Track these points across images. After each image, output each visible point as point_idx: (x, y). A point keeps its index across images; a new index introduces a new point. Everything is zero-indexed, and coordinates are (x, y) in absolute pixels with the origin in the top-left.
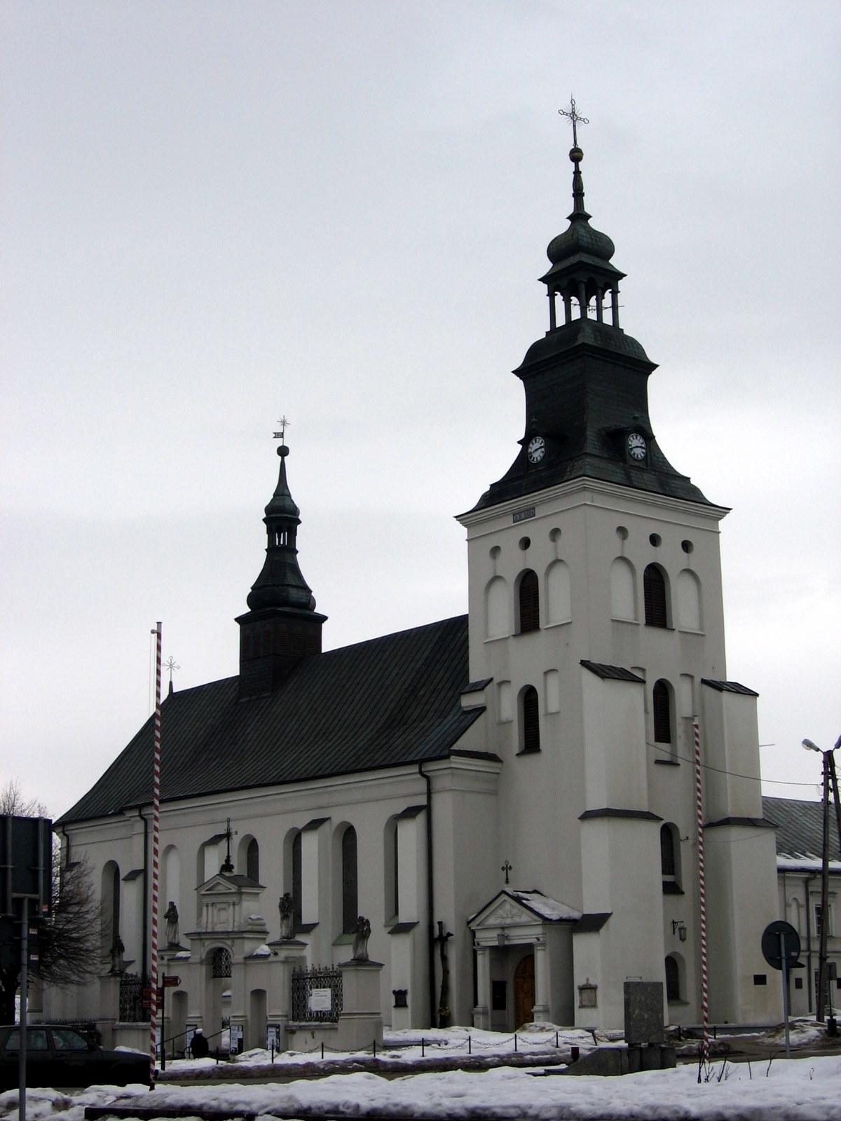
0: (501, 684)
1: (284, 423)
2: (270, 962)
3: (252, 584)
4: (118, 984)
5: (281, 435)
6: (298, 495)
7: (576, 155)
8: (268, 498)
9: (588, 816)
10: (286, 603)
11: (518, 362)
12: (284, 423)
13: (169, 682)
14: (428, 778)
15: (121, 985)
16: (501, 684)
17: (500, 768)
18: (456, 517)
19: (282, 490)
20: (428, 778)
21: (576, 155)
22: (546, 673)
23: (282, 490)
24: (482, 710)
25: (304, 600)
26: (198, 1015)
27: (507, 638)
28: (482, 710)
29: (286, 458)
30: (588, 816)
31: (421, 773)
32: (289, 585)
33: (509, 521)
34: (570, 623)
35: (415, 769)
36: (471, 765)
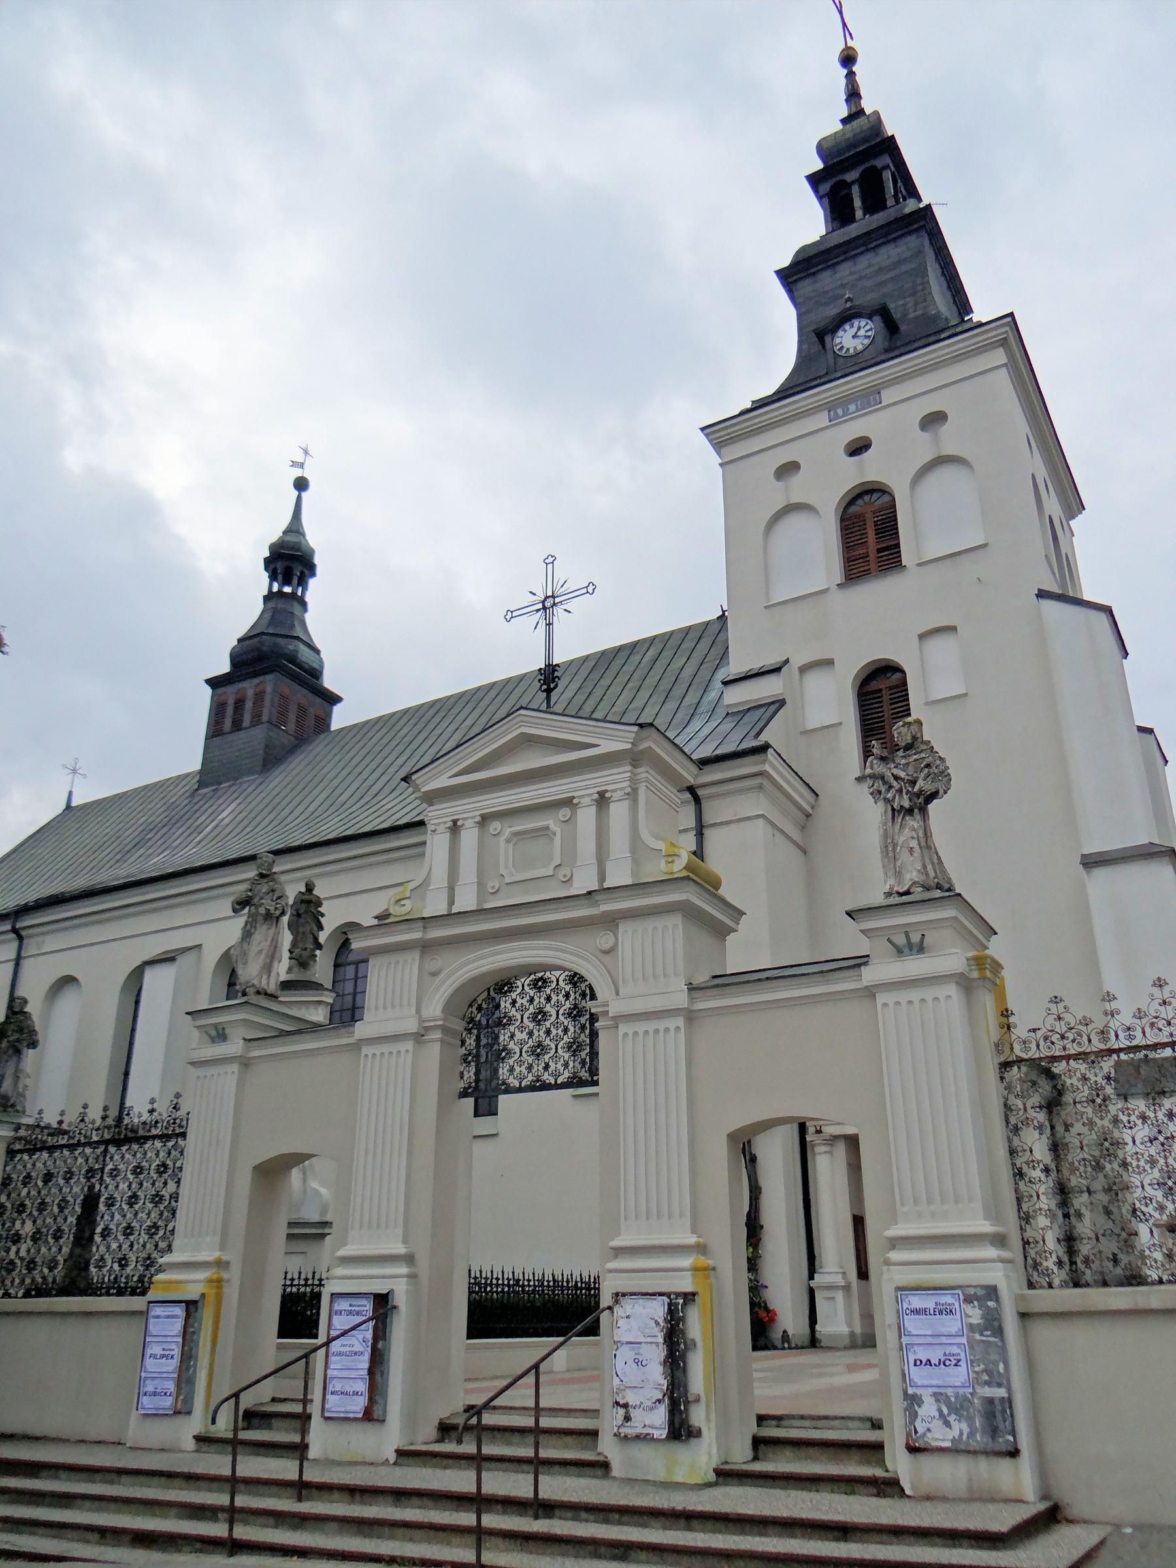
0: (804, 669)
1: (306, 452)
3: (242, 631)
5: (301, 465)
6: (314, 537)
7: (848, 59)
9: (1091, 862)
10: (293, 659)
11: (785, 262)
12: (306, 452)
13: (69, 789)
16: (804, 669)
17: (813, 808)
18: (702, 429)
20: (697, 800)
21: (848, 59)
22: (923, 637)
24: (782, 703)
25: (315, 665)
26: (400, 1249)
28: (782, 703)
29: (304, 494)
30: (1091, 862)
32: (297, 638)
33: (822, 419)
34: (985, 546)
36: (788, 782)
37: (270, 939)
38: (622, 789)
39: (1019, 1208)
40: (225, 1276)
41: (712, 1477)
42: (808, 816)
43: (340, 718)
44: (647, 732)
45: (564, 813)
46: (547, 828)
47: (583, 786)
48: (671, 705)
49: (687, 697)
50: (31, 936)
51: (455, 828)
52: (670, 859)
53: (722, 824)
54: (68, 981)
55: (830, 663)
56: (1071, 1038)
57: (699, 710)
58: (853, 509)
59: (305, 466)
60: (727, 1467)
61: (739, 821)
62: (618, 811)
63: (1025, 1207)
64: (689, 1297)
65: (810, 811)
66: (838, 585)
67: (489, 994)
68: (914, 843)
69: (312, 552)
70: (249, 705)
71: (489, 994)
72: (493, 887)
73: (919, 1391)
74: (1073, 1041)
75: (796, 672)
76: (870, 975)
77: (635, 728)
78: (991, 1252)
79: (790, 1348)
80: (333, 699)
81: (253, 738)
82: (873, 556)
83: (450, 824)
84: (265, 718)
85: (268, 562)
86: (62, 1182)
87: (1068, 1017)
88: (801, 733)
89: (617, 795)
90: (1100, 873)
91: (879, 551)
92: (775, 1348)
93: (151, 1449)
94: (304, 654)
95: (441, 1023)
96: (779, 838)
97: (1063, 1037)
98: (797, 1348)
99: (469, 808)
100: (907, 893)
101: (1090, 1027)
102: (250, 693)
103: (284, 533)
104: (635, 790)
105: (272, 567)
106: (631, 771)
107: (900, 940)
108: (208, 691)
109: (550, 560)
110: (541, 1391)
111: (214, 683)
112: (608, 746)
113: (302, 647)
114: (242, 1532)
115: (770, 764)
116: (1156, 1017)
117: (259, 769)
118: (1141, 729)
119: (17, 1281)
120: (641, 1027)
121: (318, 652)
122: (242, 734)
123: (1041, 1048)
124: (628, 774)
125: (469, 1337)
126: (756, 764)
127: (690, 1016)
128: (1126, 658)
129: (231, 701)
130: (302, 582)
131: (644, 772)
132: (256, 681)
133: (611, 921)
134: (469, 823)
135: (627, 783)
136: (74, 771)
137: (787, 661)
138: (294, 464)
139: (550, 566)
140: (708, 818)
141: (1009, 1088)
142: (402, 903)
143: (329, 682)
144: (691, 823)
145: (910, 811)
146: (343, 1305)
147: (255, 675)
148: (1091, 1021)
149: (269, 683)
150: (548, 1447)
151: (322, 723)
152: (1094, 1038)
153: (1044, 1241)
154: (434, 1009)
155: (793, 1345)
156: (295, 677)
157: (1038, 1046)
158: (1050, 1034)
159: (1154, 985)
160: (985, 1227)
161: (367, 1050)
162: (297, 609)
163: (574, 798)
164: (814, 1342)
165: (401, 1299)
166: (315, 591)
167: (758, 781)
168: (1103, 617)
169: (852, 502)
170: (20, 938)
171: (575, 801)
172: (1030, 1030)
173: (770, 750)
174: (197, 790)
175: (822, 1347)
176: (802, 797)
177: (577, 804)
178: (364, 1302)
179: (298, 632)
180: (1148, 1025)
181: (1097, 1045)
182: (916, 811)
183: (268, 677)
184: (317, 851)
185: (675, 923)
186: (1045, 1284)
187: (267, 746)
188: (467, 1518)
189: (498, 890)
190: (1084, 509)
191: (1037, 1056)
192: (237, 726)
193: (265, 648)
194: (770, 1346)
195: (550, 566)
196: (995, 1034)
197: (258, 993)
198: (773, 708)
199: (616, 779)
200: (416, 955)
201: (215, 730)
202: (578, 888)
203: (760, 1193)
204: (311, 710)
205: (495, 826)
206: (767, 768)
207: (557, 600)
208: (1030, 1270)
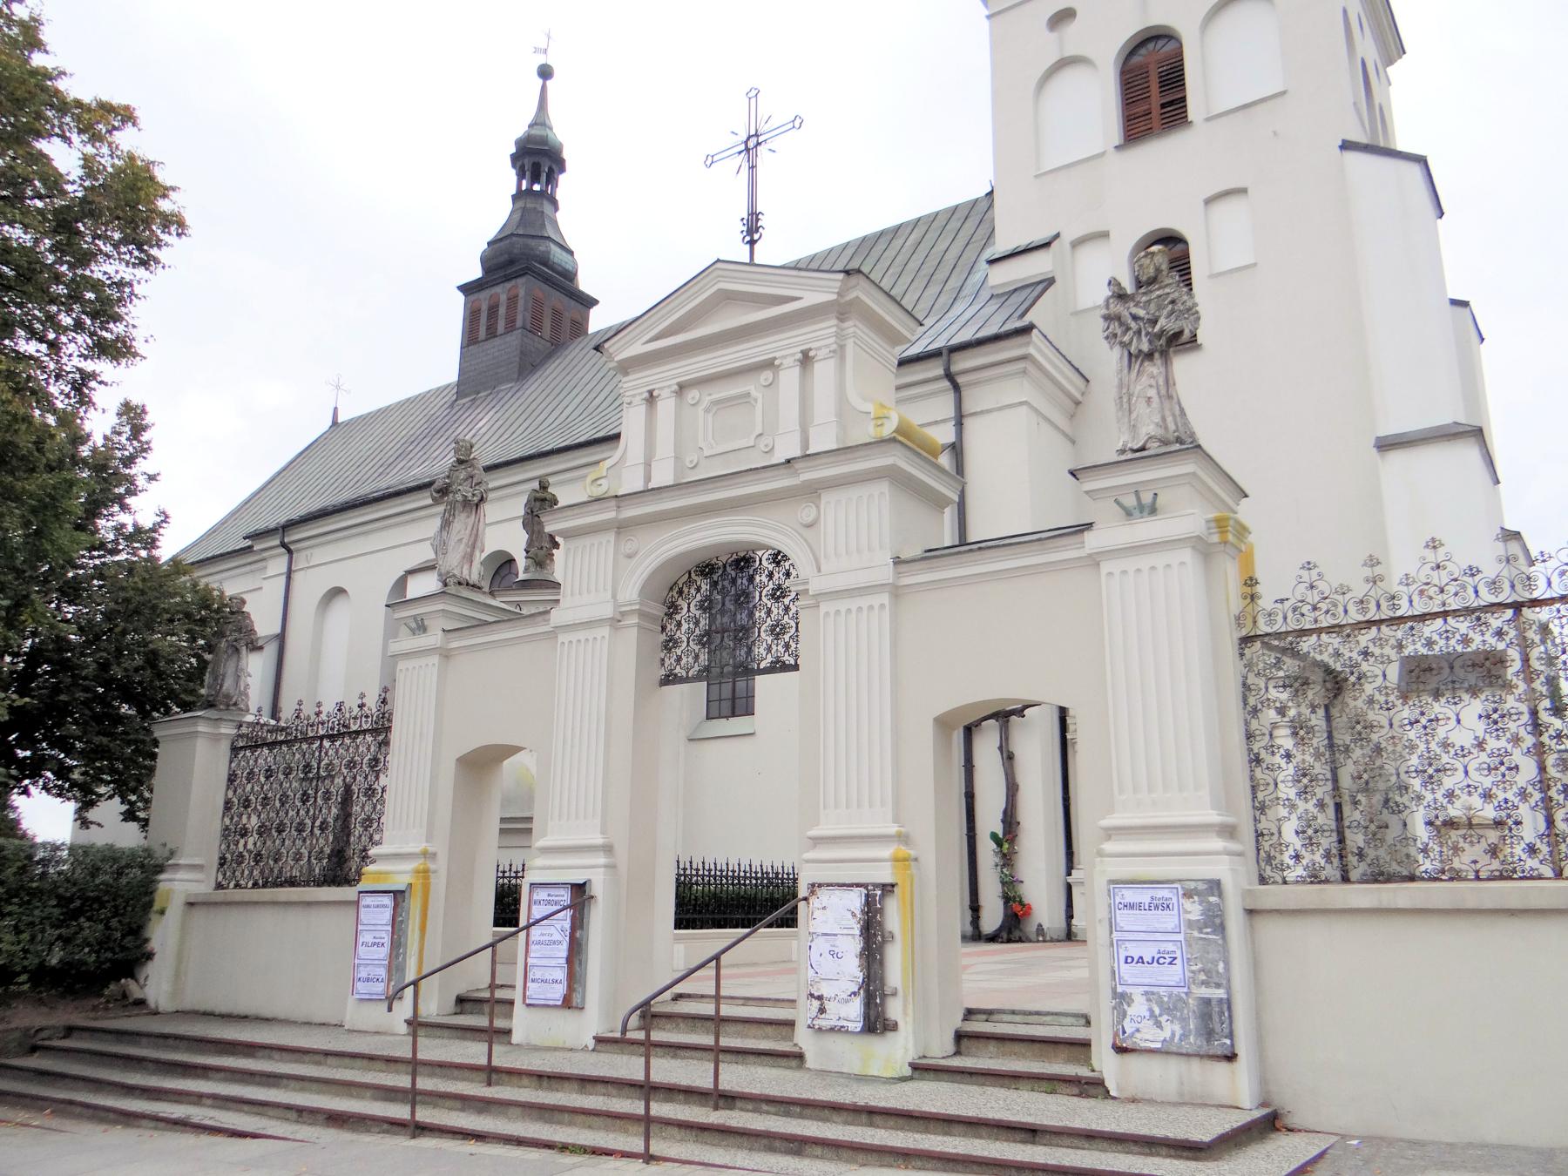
0: (1076, 244)
3: (492, 232)
4: (225, 747)
8: (520, 129)
9: (1385, 445)
10: (545, 261)
14: (956, 388)
15: (235, 750)
17: (1083, 394)
19: (541, 120)
20: (956, 388)
22: (1208, 202)
23: (541, 120)
24: (1050, 281)
25: (569, 267)
26: (599, 840)
27: (1103, 154)
28: (1050, 281)
29: (548, 82)
30: (1385, 445)
31: (949, 376)
32: (548, 238)
34: (1284, 93)
35: (936, 369)
36: (1056, 367)
37: (469, 528)
38: (827, 346)
39: (1254, 797)
40: (432, 866)
41: (907, 1071)
42: (1078, 403)
43: (597, 321)
44: (854, 279)
45: (766, 376)
46: (748, 395)
47: (784, 346)
48: (933, 290)
49: (949, 282)
50: (298, 550)
51: (651, 398)
52: (880, 422)
53: (982, 412)
54: (337, 592)
55: (1104, 235)
56: (1325, 609)
57: (963, 294)
58: (1136, 59)
59: (548, 52)
60: (924, 1061)
61: (1000, 409)
62: (824, 370)
63: (1260, 796)
64: (888, 888)
65: (1078, 395)
66: (1116, 147)
67: (690, 577)
68: (1152, 393)
69: (561, 145)
70: (502, 311)
71: (690, 577)
72: (691, 462)
73: (1129, 990)
74: (1327, 612)
75: (1068, 246)
76: (1092, 541)
77: (841, 276)
78: (1218, 844)
79: (1044, 941)
80: (589, 302)
81: (508, 345)
82: (1156, 111)
83: (646, 395)
84: (519, 323)
85: (515, 159)
86: (281, 777)
87: (1321, 585)
88: (1072, 314)
90: (1397, 458)
91: (1163, 106)
92: (1030, 941)
93: (366, 1032)
94: (557, 255)
95: (637, 607)
96: (1045, 426)
97: (1315, 608)
98: (1052, 940)
99: (665, 377)
100: (1143, 449)
101: (1348, 596)
102: (503, 298)
103: (530, 126)
104: (842, 347)
105: (519, 164)
106: (836, 326)
107: (1130, 501)
108: (461, 297)
109: (753, 93)
110: (722, 982)
111: (466, 289)
112: (811, 298)
113: (554, 248)
114: (425, 1115)
115: (1035, 346)
116: (1428, 584)
117: (516, 376)
118: (1454, 302)
119: (246, 872)
120: (843, 605)
121: (571, 253)
122: (497, 341)
123: (1289, 620)
124: (834, 329)
125: (496, 924)
126: (1020, 346)
127: (896, 592)
128: (1441, 217)
129: (484, 307)
130: (551, 179)
131: (853, 327)
132: (508, 285)
133: (812, 491)
134: (665, 393)
135: (834, 339)
136: (338, 387)
137: (1057, 236)
138: (536, 50)
139: (753, 100)
140: (968, 407)
141: (1249, 666)
142: (599, 482)
143: (585, 284)
144: (950, 411)
145: (1149, 356)
146: (541, 895)
147: (508, 279)
148: (1349, 590)
149: (522, 286)
150: (728, 1035)
151: (579, 327)
152: (1352, 609)
153: (1280, 833)
154: (630, 592)
155: (1048, 938)
156: (547, 280)
157: (1285, 618)
158: (1300, 604)
159: (1427, 546)
160: (1214, 817)
161: (562, 638)
162: (547, 208)
163: (775, 358)
164: (1069, 936)
165: (597, 889)
166: (566, 187)
167: (1021, 365)
168: (1415, 170)
169: (1132, 53)
170: (290, 552)
171: (777, 362)
172: (1276, 601)
173: (1035, 331)
174: (456, 400)
175: (1077, 941)
176: (1072, 384)
177: (779, 366)
178: (562, 892)
179: (550, 232)
180: (1417, 592)
181: (1355, 616)
182: (1157, 355)
183: (520, 281)
184: (570, 455)
185: (881, 492)
186: (1280, 880)
187: (522, 352)
188: (636, 1107)
189: (697, 464)
190: (1404, 53)
191: (1283, 630)
192: (492, 333)
193: (516, 251)
194: (1024, 939)
195: (753, 100)
196: (1237, 604)
197: (460, 583)
198: (1040, 287)
199: (820, 335)
200: (610, 537)
201: (471, 338)
202: (779, 457)
203: (1017, 790)
204: (566, 314)
205: (693, 395)
206: (1032, 350)
207: (761, 139)
208: (1263, 864)
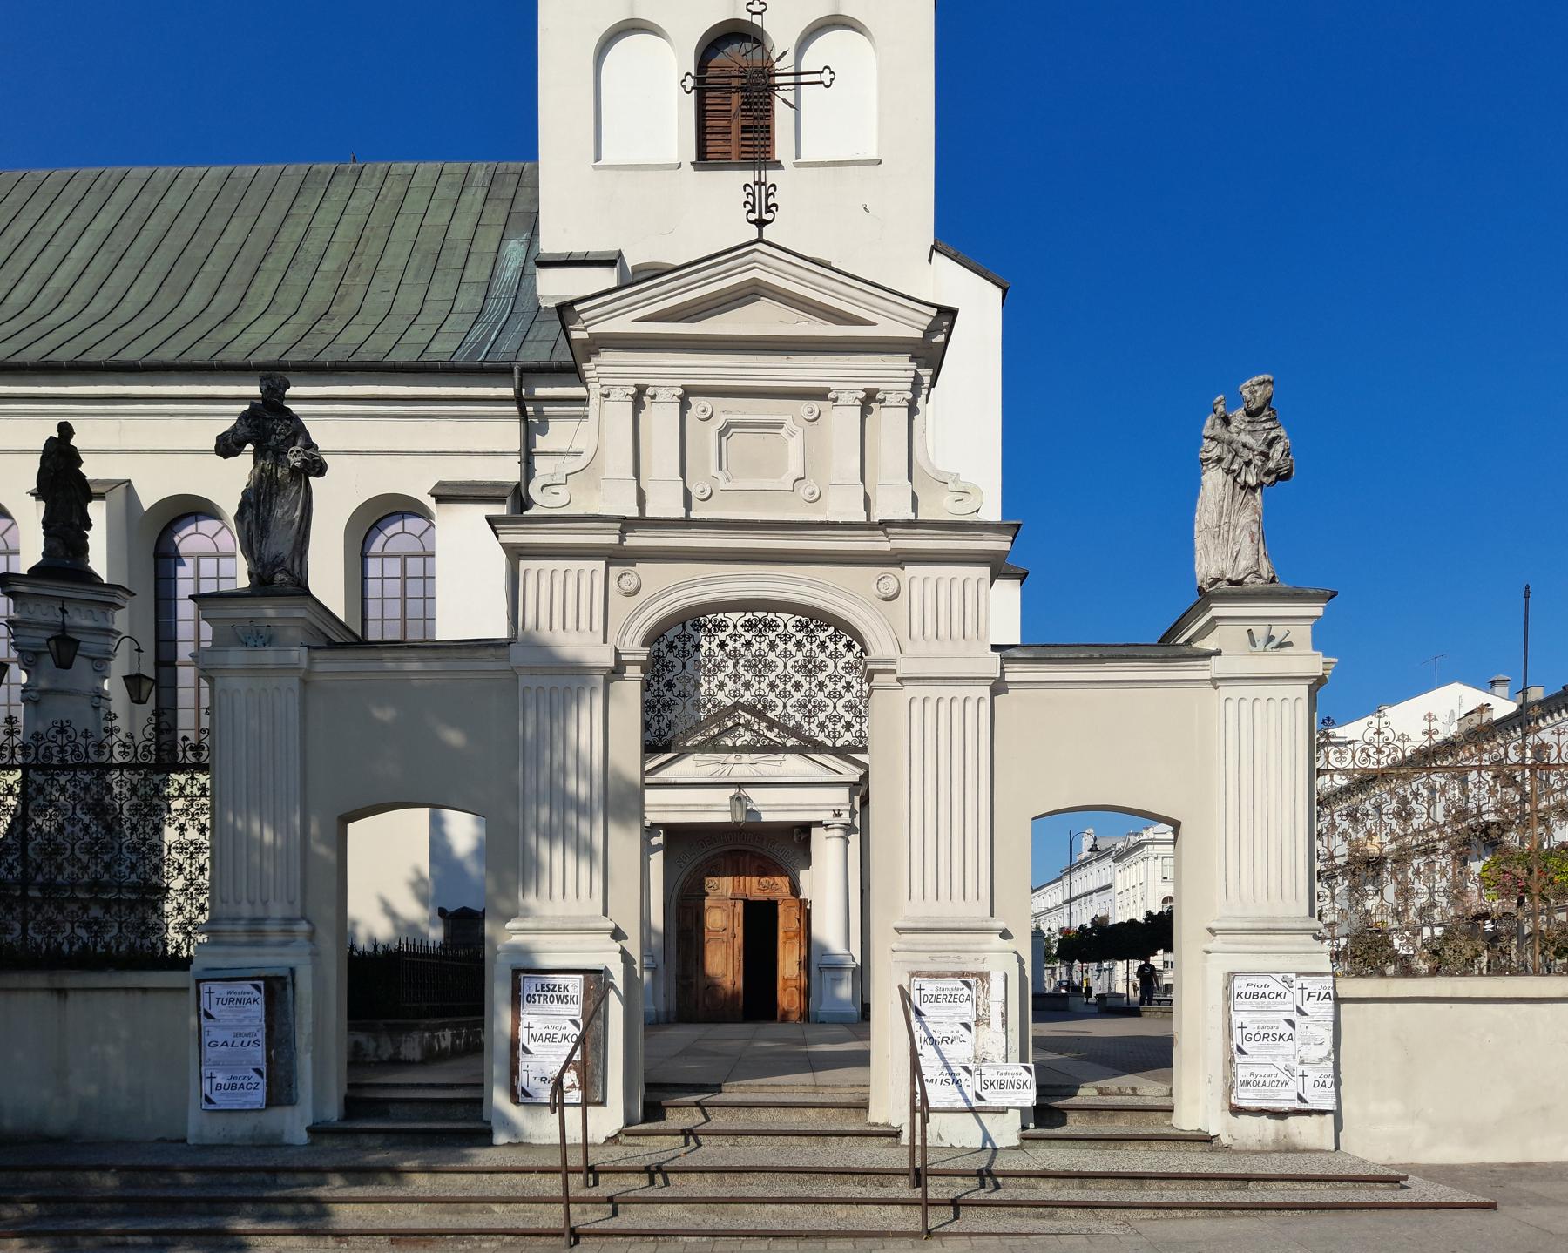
2: (1214, 682)
38: (899, 392)
51: (639, 398)
52: (960, 496)
56: (1387, 752)
83: (633, 391)
87: (1388, 733)
89: (891, 399)
97: (1379, 751)
100: (1240, 582)
101: (1407, 744)
120: (933, 691)
123: (1356, 759)
127: (998, 687)
134: (663, 395)
142: (554, 489)
148: (1408, 739)
157: (1353, 757)
158: (1368, 747)
171: (831, 396)
177: (835, 400)
189: (711, 494)
191: (1351, 766)
